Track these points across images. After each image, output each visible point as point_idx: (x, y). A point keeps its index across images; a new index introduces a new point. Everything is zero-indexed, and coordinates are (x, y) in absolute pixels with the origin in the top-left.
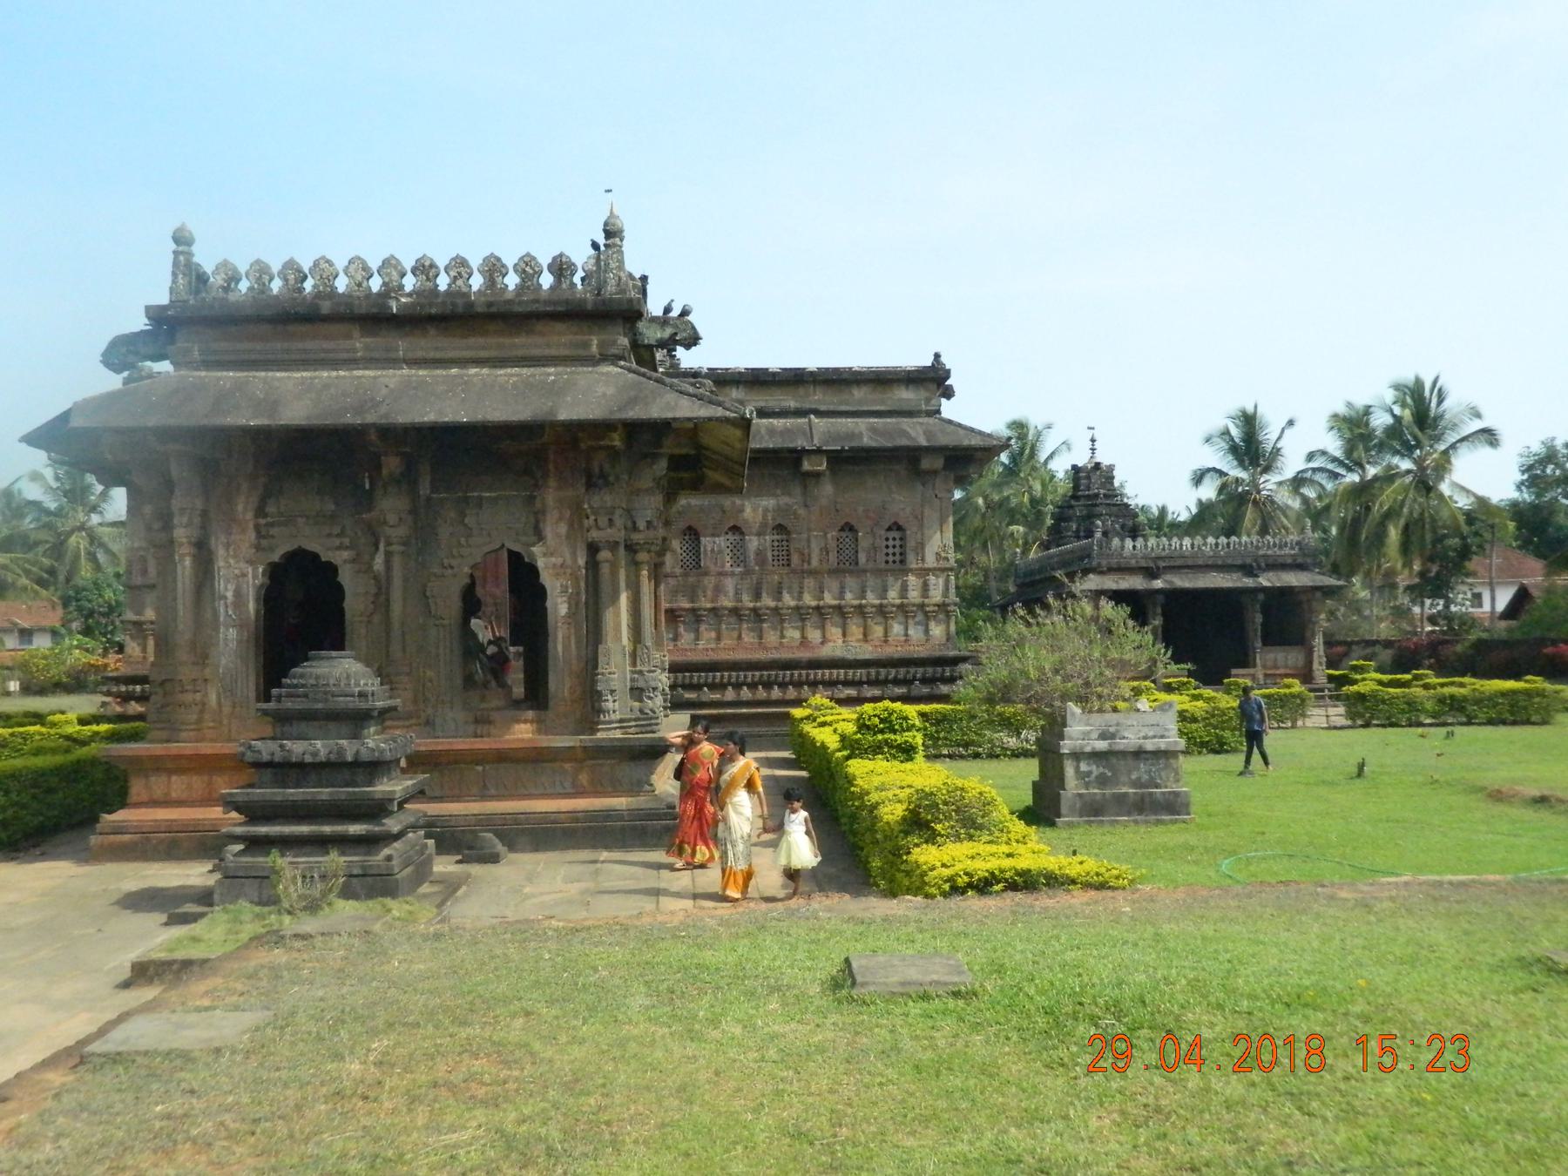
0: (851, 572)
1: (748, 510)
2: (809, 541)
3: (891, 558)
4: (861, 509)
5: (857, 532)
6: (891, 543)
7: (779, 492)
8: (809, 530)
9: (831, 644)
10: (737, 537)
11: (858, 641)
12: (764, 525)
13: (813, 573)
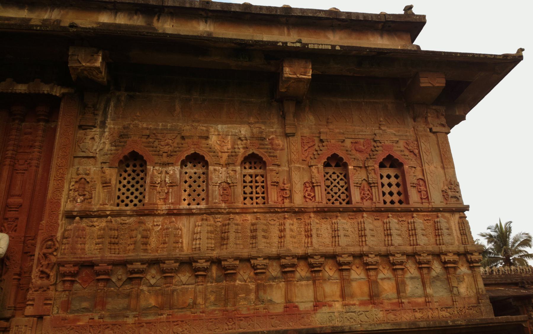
0: (345, 211)
1: (214, 140)
2: (289, 172)
3: (388, 198)
4: (348, 143)
5: (345, 165)
6: (386, 181)
7: (252, 120)
8: (289, 162)
9: (325, 309)
10: (199, 170)
11: (363, 303)
12: (233, 155)
13: (298, 212)
